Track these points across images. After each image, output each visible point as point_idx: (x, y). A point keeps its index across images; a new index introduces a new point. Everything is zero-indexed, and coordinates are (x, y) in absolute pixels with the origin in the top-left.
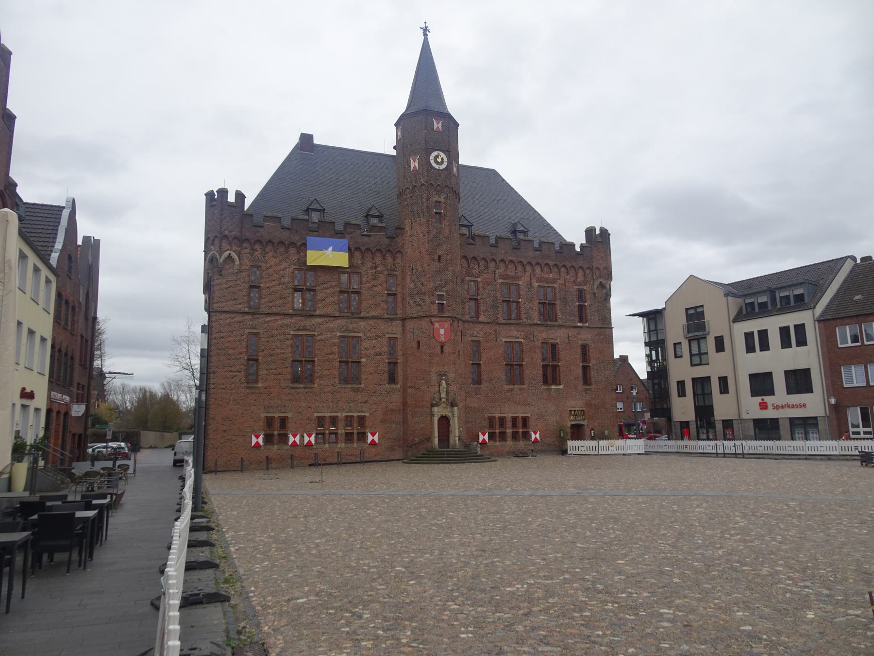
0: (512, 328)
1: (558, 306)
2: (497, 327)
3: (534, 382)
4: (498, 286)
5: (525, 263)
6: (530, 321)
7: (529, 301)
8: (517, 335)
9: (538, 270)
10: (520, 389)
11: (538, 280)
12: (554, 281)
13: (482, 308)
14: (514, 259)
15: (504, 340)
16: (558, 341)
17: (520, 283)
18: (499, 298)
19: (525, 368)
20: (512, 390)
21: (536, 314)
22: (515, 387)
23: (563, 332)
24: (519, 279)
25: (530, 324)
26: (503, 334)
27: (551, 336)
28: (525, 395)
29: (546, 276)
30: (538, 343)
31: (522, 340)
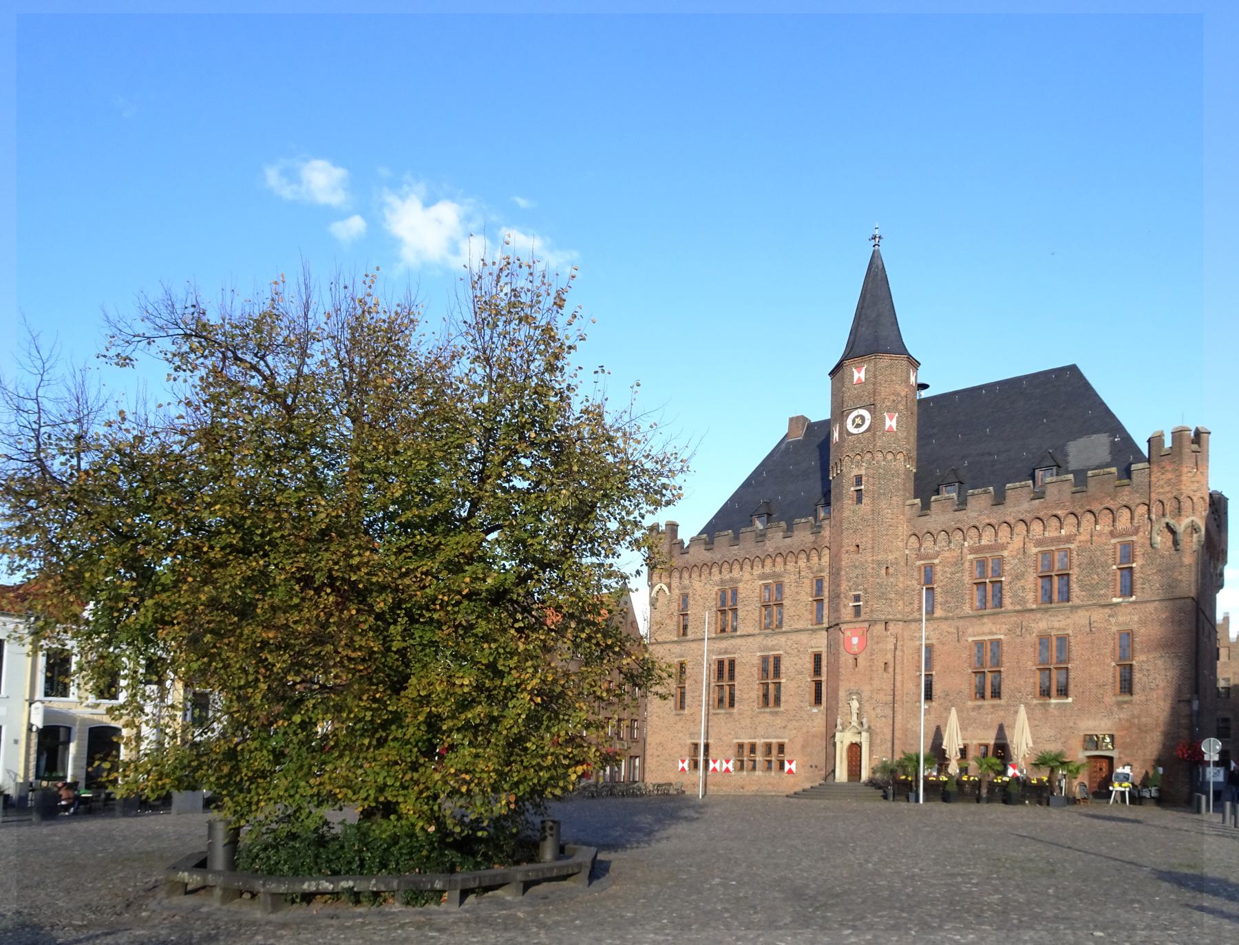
0: (985, 620)
1: (1073, 578)
2: (961, 623)
3: (1018, 695)
4: (967, 564)
5: (1012, 521)
6: (1018, 608)
7: (1018, 577)
8: (990, 629)
9: (1037, 527)
10: (993, 706)
11: (1039, 543)
12: (1069, 539)
13: (939, 599)
14: (993, 521)
15: (970, 639)
16: (1070, 632)
17: (1005, 553)
18: (967, 579)
19: (1003, 675)
20: (980, 707)
21: (1030, 596)
22: (986, 703)
23: (1081, 617)
24: (1003, 547)
25: (1018, 612)
26: (970, 630)
27: (1056, 625)
28: (1002, 713)
29: (1054, 534)
30: (1032, 638)
31: (1002, 637)
